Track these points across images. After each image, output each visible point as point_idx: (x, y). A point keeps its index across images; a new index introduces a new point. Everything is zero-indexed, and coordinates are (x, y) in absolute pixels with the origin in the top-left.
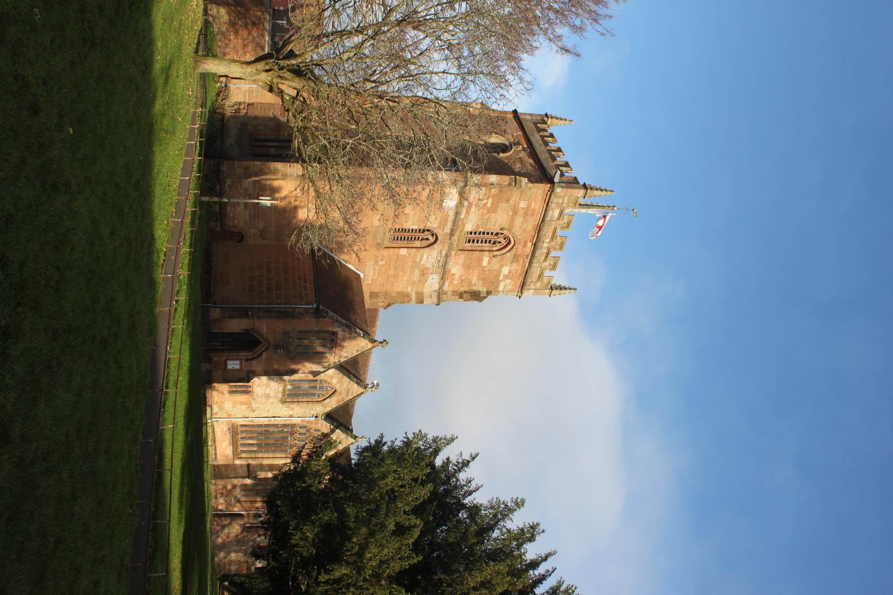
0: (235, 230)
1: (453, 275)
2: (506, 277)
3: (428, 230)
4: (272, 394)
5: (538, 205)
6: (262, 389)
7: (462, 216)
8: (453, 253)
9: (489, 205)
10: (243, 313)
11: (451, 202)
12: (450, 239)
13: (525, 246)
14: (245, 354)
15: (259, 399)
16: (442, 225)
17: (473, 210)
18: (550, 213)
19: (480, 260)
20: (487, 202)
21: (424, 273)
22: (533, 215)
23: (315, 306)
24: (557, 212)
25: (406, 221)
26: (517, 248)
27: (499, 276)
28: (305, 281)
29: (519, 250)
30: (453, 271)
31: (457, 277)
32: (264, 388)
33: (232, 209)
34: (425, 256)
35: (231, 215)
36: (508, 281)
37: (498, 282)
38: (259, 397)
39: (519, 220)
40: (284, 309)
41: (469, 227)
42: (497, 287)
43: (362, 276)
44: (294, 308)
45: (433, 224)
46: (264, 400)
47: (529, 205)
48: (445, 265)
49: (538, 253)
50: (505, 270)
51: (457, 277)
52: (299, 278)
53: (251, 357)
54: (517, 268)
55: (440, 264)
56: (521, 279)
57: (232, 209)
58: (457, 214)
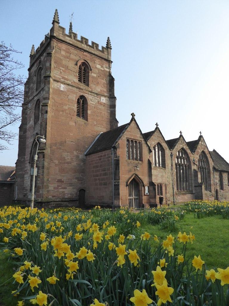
0: (78, 194)
1: (101, 90)
2: (102, 67)
3: (78, 100)
4: (161, 174)
5: (64, 46)
6: (159, 179)
7: (70, 83)
8: (90, 89)
9: (63, 69)
10: (117, 187)
11: (62, 87)
12: (82, 89)
13: (86, 56)
14: (141, 187)
15: (164, 180)
16: (73, 92)
17: (66, 77)
18: (68, 41)
19: (93, 77)
20: (62, 70)
21: (99, 103)
22: (69, 49)
23: (112, 149)
24: (67, 38)
25: (73, 109)
26: (87, 59)
27: (101, 70)
28: (101, 156)
29: (88, 59)
30: (100, 90)
31: (102, 89)
32: (158, 178)
33: (66, 195)
34: (92, 102)
35: (69, 195)
36: (104, 66)
37: (104, 71)
38: (163, 181)
39: (72, 56)
40: (115, 165)
41: (76, 80)
42: (107, 72)
43: (102, 133)
44: (114, 160)
45: (74, 98)
46: (164, 178)
47: (64, 50)
48: (97, 94)
49: (90, 51)
50: (99, 66)
51: (102, 89)
52: (100, 159)
53: (142, 183)
54: (97, 61)
55: (96, 96)
56: (103, 60)
57: (66, 195)
58: (68, 85)
